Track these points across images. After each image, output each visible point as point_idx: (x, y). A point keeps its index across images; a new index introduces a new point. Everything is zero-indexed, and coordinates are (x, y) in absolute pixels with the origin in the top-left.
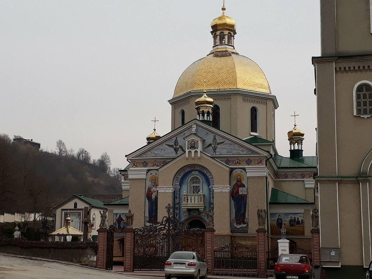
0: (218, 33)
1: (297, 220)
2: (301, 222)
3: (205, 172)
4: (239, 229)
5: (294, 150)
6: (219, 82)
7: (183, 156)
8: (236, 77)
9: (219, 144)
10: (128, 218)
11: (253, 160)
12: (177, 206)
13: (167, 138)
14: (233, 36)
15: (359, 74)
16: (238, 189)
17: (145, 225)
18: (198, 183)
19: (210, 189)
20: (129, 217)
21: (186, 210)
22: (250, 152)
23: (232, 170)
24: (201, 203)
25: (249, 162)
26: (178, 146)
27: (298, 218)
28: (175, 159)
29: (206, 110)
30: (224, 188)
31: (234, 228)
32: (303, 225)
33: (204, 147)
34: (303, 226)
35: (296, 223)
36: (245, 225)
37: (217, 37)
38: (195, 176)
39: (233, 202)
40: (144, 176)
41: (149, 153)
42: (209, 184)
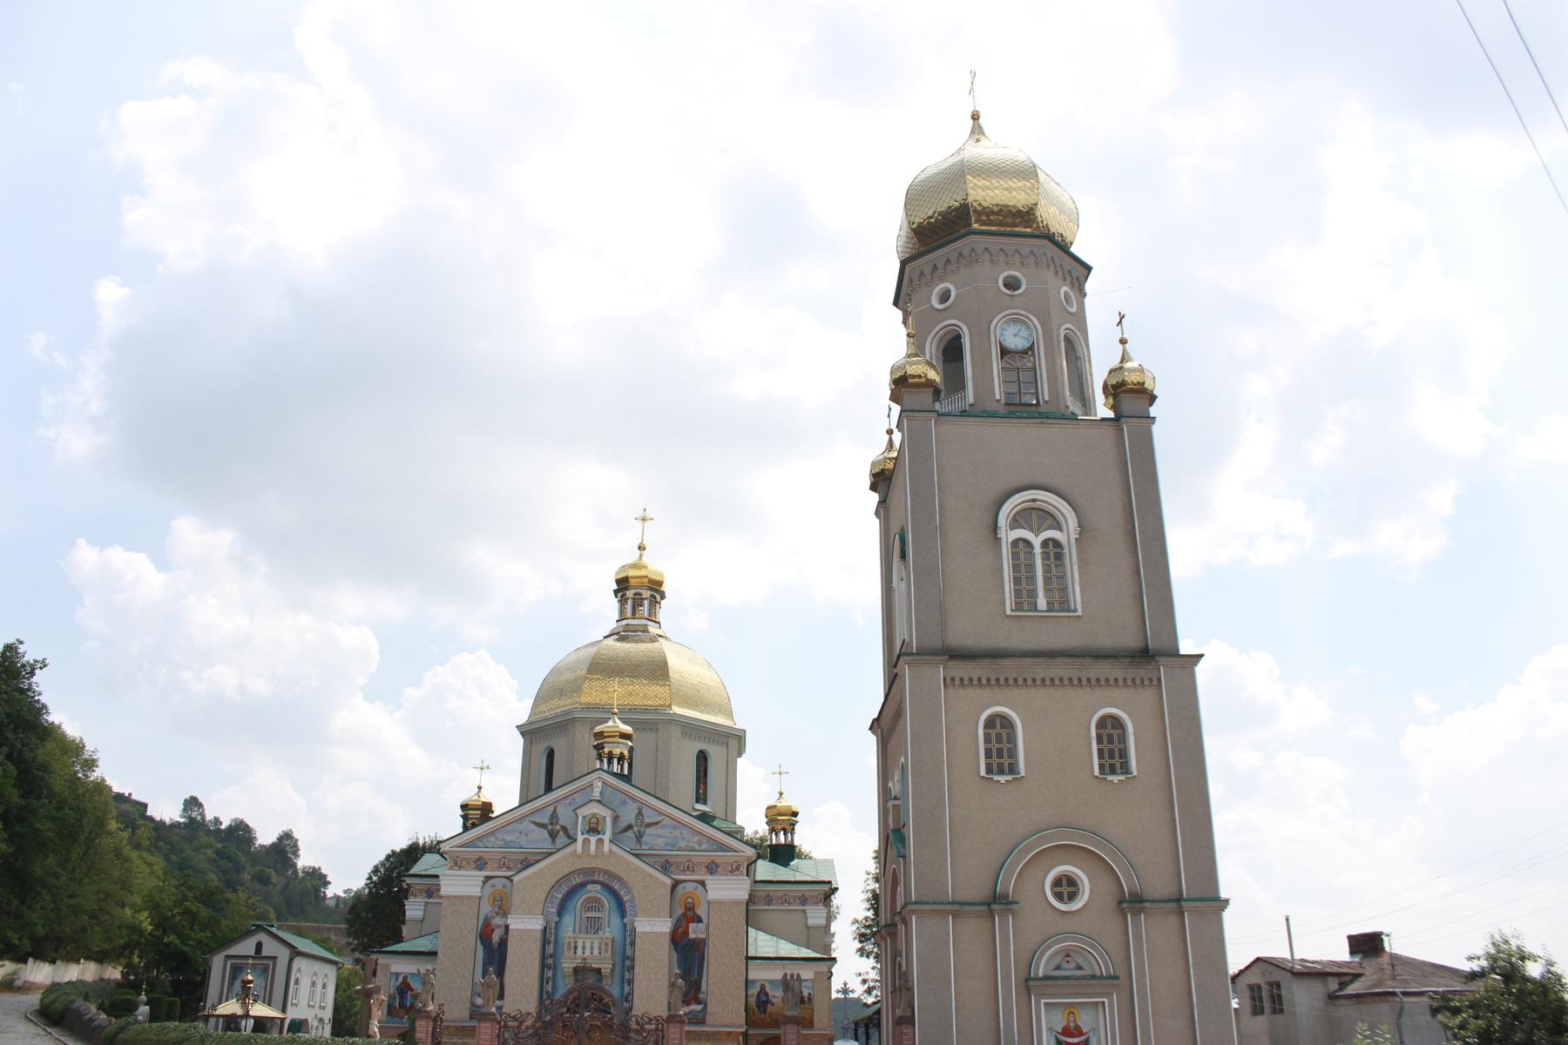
0: (630, 593)
2: (806, 999)
3: (616, 887)
9: (649, 825)
10: (486, 987)
11: (723, 863)
12: (550, 961)
14: (660, 603)
15: (987, 692)
16: (687, 927)
17: (473, 1004)
18: (599, 911)
19: (625, 925)
21: (571, 970)
22: (715, 847)
23: (676, 884)
25: (712, 868)
26: (558, 827)
28: (551, 854)
29: (617, 751)
32: (810, 1007)
33: (616, 832)
34: (810, 1007)
36: (699, 1007)
38: (593, 894)
39: (675, 955)
40: (475, 890)
41: (492, 839)
42: (623, 915)
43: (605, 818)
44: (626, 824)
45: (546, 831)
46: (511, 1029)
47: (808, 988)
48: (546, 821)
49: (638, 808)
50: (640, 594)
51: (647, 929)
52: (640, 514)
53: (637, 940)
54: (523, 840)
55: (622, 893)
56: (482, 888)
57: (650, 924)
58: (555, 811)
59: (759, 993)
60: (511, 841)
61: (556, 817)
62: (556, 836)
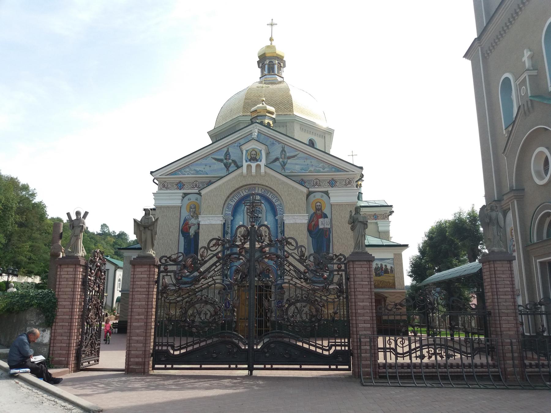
0: (267, 62)
1: (384, 267)
2: (389, 271)
3: (270, 197)
7: (238, 172)
9: (289, 158)
10: (142, 228)
13: (214, 148)
16: (318, 222)
19: (277, 220)
20: (145, 228)
22: (333, 169)
25: (332, 183)
27: (386, 266)
33: (269, 162)
37: (265, 67)
40: (178, 203)
41: (187, 170)
42: (275, 213)
43: (261, 151)
44: (274, 157)
46: (172, 274)
47: (390, 263)
48: (223, 157)
49: (282, 147)
50: (272, 62)
52: (269, 22)
53: (286, 229)
54: (207, 169)
55: (274, 201)
56: (182, 200)
57: (293, 218)
58: (228, 151)
60: (200, 171)
61: (229, 154)
62: (229, 166)
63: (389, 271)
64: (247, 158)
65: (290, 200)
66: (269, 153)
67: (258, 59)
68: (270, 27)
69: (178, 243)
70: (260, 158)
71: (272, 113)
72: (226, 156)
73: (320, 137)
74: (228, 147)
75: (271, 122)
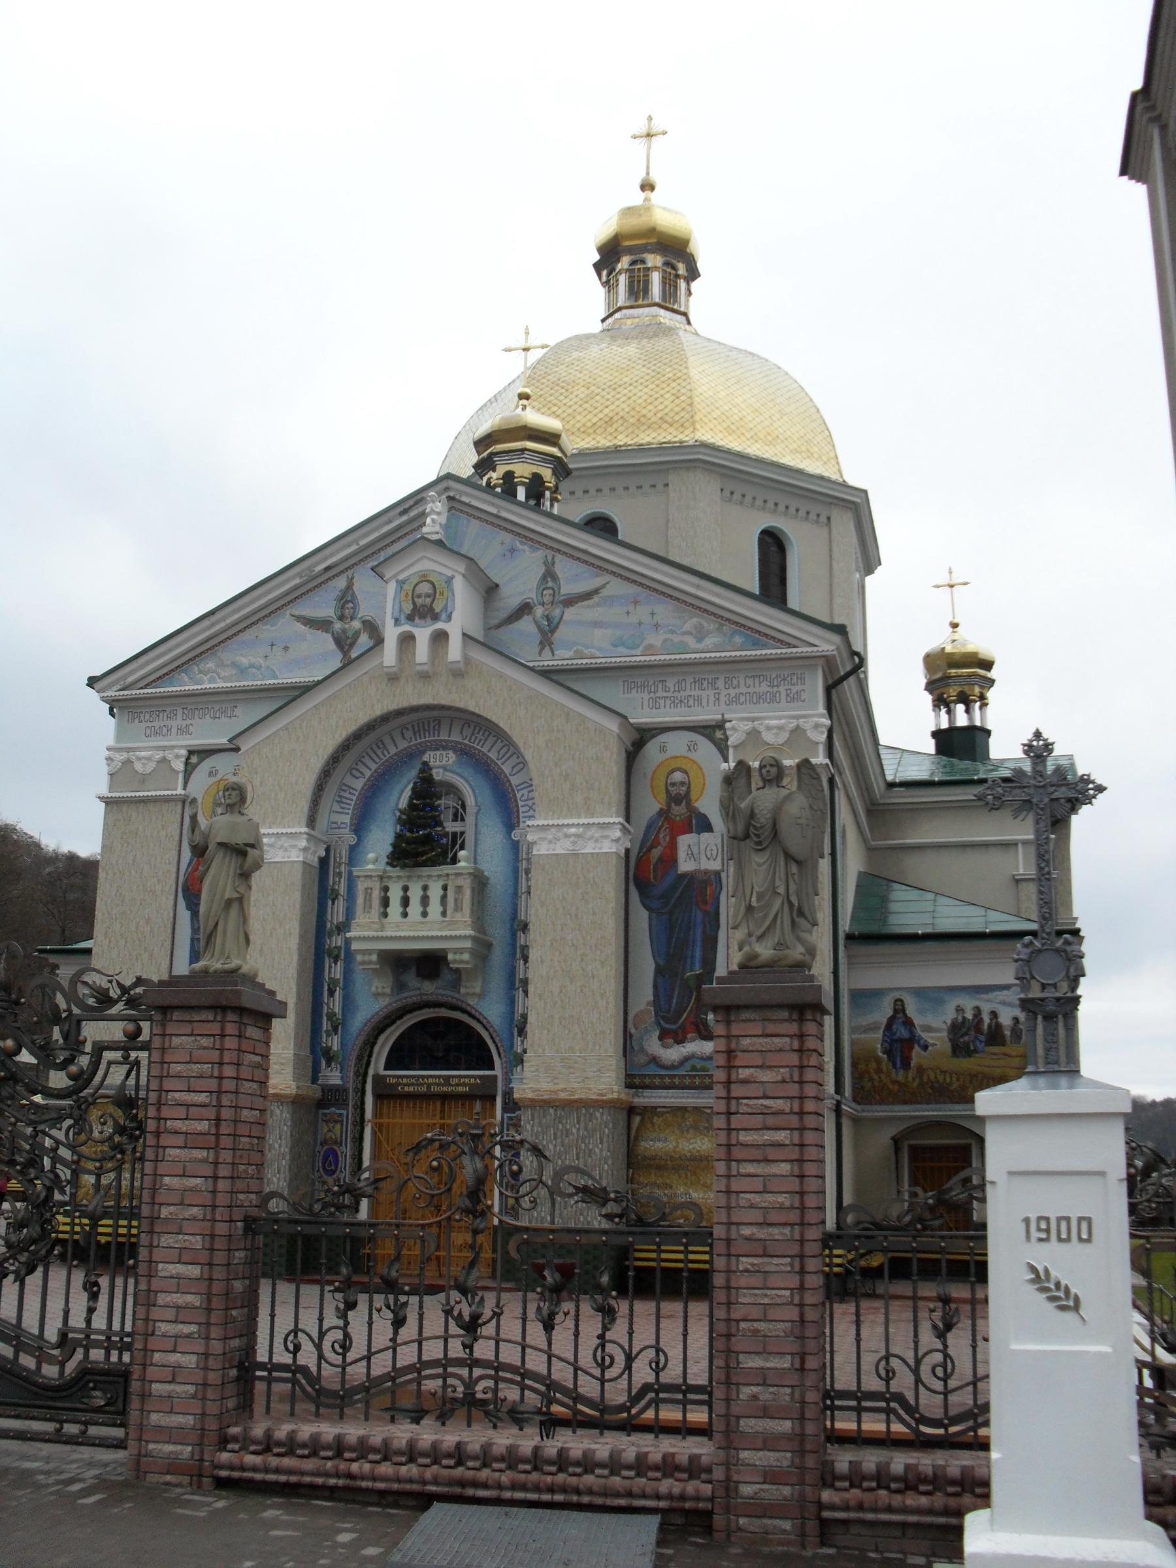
0: (624, 262)
2: (1007, 1033)
3: (493, 755)
4: (673, 1067)
5: (953, 730)
6: (615, 418)
8: (690, 397)
12: (337, 941)
16: (673, 846)
21: (374, 957)
22: (738, 640)
24: (458, 917)
26: (356, 624)
27: (994, 1014)
29: (523, 470)
30: (592, 832)
31: (649, 1063)
33: (496, 622)
35: (982, 1038)
39: (641, 917)
41: (210, 665)
42: (510, 818)
43: (449, 580)
44: (515, 602)
45: (328, 637)
47: (1010, 1005)
49: (545, 563)
51: (562, 847)
55: (506, 769)
57: (567, 836)
58: (350, 587)
59: (891, 1020)
60: (252, 666)
61: (353, 600)
62: (352, 645)
63: (1003, 1037)
64: (401, 610)
65: (556, 765)
66: (497, 586)
67: (596, 257)
68: (641, 144)
69: (170, 931)
70: (445, 608)
71: (551, 438)
72: (343, 607)
73: (817, 522)
74: (350, 573)
75: (547, 473)
